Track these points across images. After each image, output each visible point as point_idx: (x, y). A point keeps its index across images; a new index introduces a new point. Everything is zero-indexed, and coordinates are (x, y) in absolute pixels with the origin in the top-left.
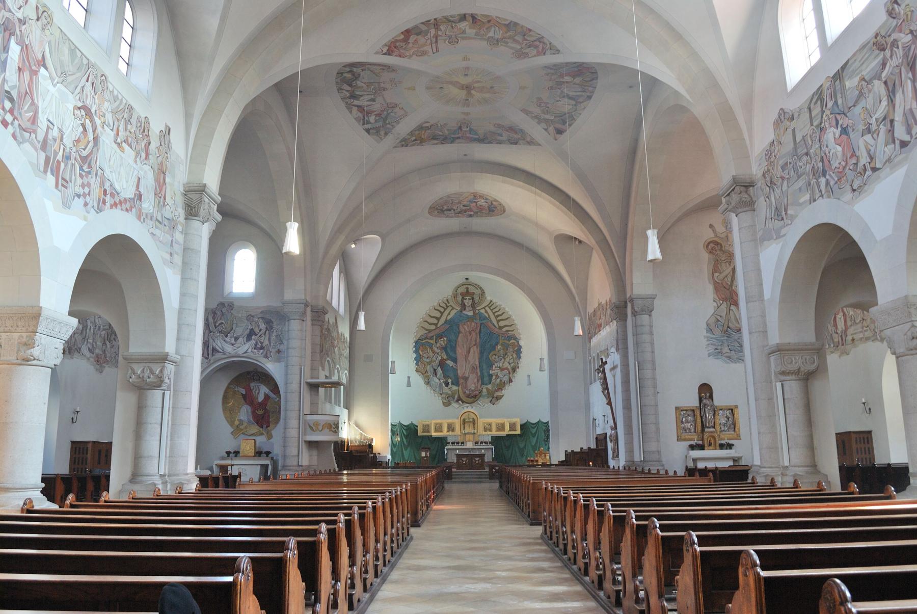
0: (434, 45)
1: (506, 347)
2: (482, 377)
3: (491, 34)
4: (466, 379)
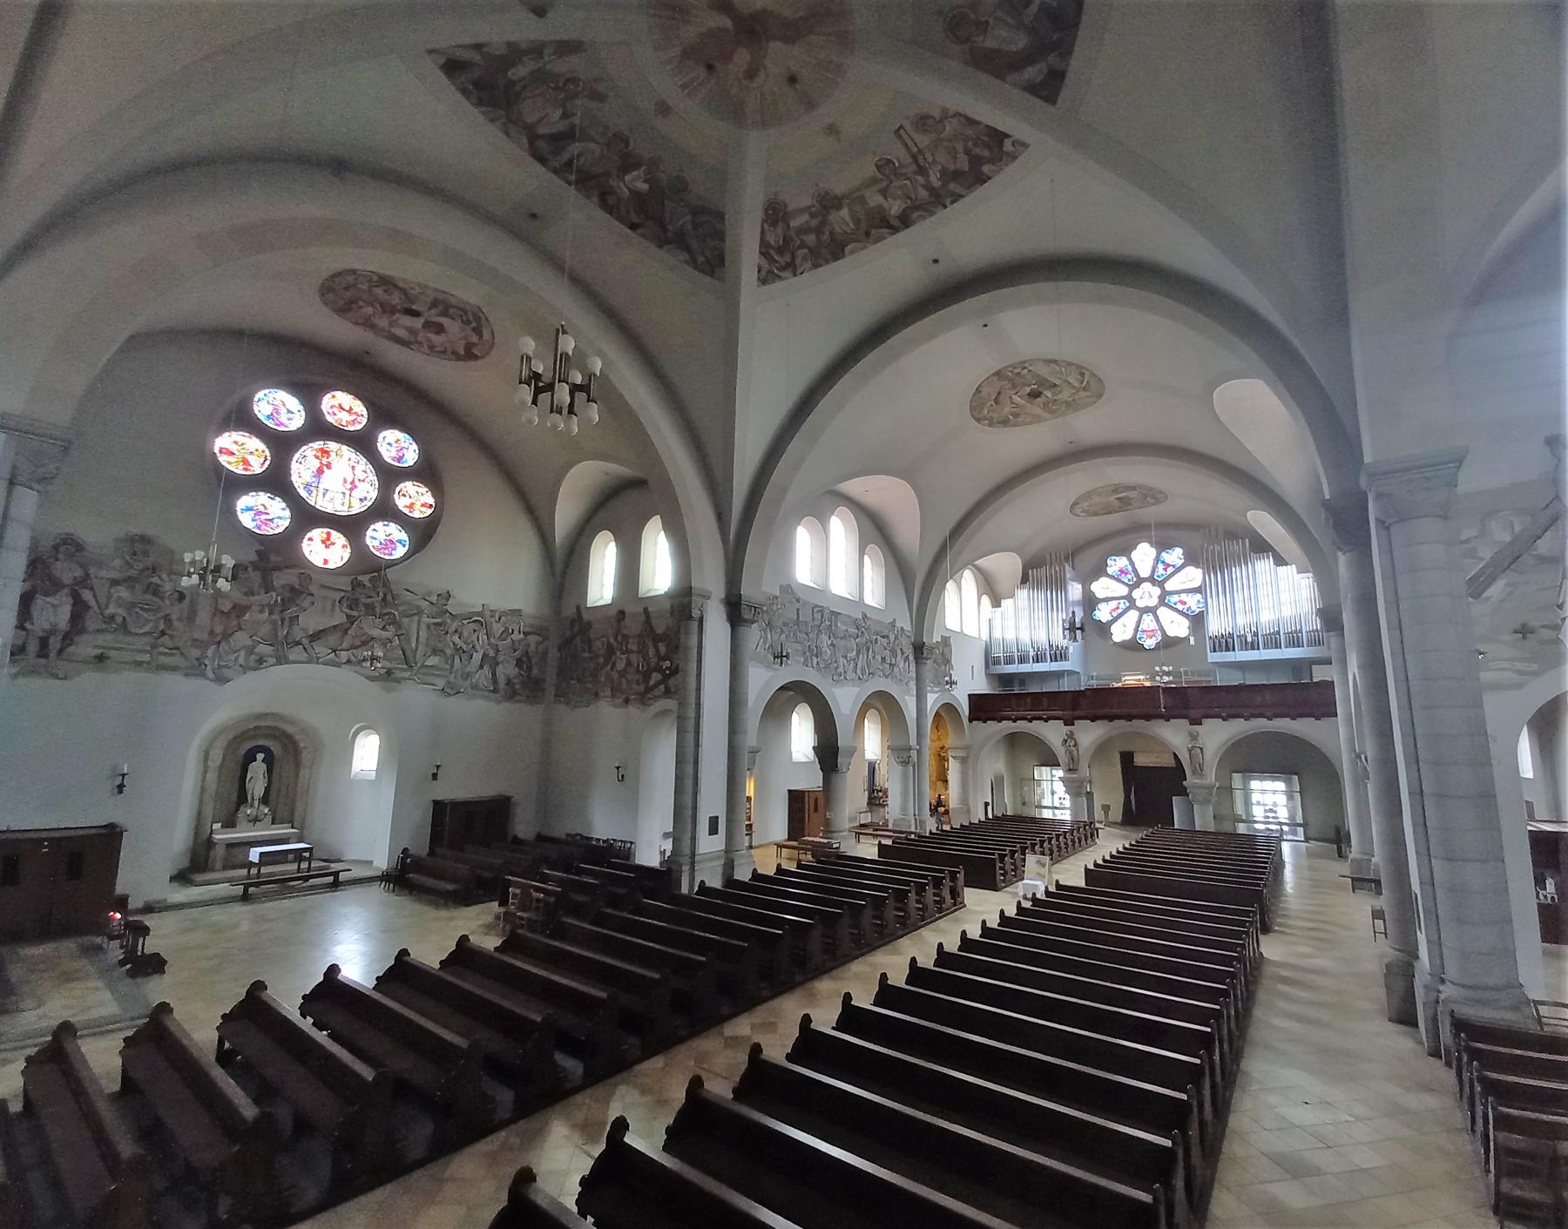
0: (915, 149)
3: (845, 212)
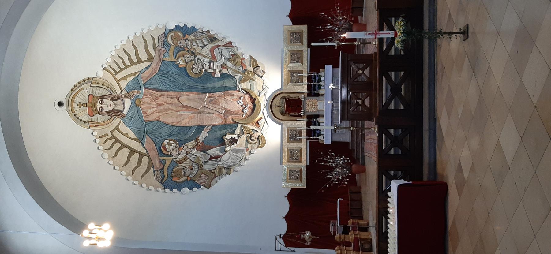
1: (179, 50)
2: (225, 89)
4: (228, 112)
